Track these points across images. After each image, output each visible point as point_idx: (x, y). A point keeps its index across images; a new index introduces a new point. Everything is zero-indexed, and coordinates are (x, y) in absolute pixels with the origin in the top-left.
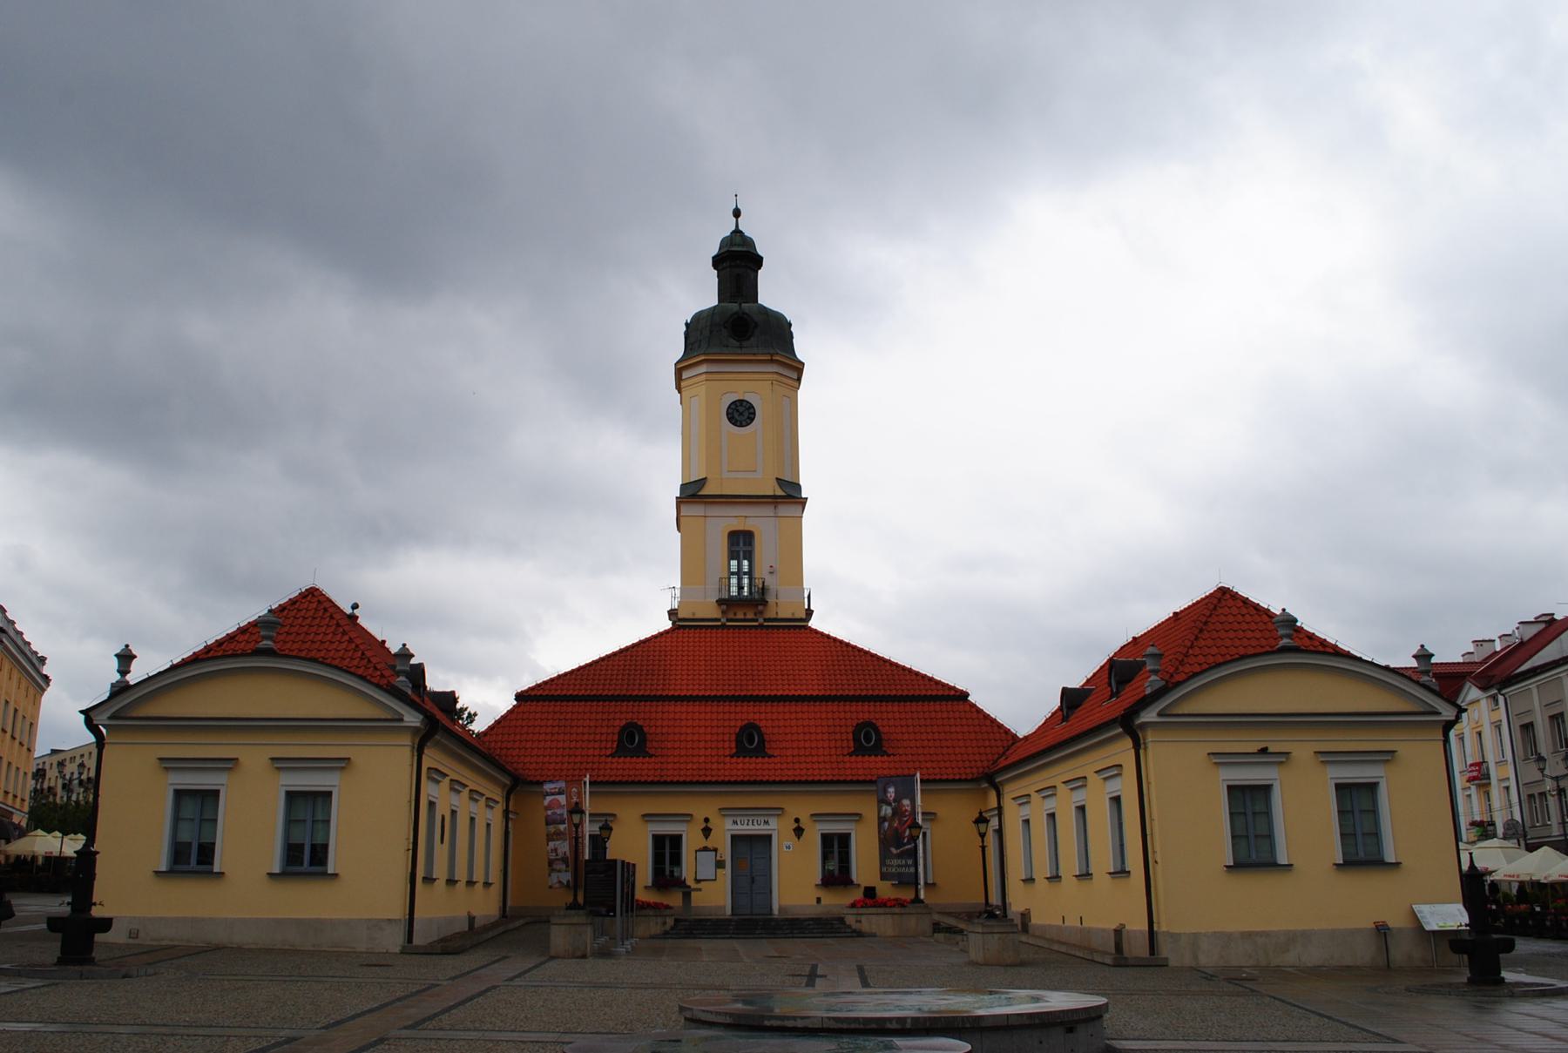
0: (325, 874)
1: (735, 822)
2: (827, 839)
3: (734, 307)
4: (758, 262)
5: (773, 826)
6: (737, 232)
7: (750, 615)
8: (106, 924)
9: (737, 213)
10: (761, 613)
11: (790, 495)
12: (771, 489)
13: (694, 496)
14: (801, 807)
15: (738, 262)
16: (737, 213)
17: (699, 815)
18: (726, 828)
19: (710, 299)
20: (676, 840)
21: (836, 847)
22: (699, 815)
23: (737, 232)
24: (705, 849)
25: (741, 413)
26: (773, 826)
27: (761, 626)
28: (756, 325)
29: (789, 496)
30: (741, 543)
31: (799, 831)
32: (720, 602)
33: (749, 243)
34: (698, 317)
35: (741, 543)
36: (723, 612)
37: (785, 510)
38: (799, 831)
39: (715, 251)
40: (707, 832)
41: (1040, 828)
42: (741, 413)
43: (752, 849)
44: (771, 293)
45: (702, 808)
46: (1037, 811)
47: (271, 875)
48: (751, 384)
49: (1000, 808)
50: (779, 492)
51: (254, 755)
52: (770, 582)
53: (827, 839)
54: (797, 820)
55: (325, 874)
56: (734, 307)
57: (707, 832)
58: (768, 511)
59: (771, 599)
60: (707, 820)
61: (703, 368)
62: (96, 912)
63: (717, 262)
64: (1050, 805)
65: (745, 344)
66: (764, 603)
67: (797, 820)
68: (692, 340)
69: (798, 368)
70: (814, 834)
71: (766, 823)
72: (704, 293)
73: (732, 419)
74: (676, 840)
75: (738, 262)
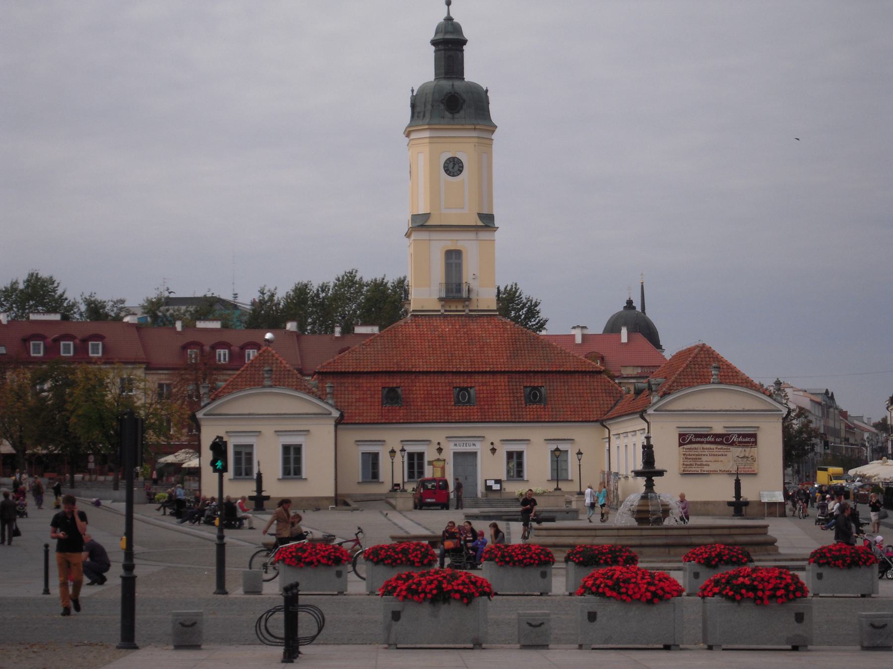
0: (301, 479)
1: (456, 445)
2: (510, 455)
4: (464, 42)
6: (449, 19)
7: (460, 308)
8: (268, 498)
10: (467, 306)
11: (487, 222)
12: (475, 221)
13: (422, 226)
14: (495, 434)
15: (450, 45)
17: (435, 441)
18: (450, 449)
20: (421, 455)
21: (516, 460)
22: (435, 441)
23: (449, 19)
24: (438, 460)
25: (454, 167)
27: (467, 316)
28: (464, 101)
29: (487, 226)
30: (453, 258)
31: (493, 450)
32: (441, 299)
33: (457, 29)
34: (422, 89)
35: (453, 258)
36: (443, 306)
37: (484, 235)
38: (493, 450)
39: (432, 36)
40: (440, 450)
41: (622, 449)
42: (454, 167)
43: (466, 459)
44: (474, 71)
45: (437, 434)
47: (279, 479)
48: (461, 144)
49: (609, 438)
50: (480, 223)
51: (268, 429)
52: (474, 285)
53: (510, 455)
54: (492, 444)
55: (301, 479)
56: (446, 84)
57: (440, 450)
58: (471, 236)
59: (473, 296)
60: (439, 444)
61: (427, 134)
62: (264, 494)
63: (434, 43)
64: (626, 441)
65: (457, 115)
66: (469, 299)
67: (492, 444)
68: (418, 109)
69: (492, 128)
71: (474, 445)
72: (423, 70)
73: (447, 171)
74: (421, 455)
75: (450, 45)
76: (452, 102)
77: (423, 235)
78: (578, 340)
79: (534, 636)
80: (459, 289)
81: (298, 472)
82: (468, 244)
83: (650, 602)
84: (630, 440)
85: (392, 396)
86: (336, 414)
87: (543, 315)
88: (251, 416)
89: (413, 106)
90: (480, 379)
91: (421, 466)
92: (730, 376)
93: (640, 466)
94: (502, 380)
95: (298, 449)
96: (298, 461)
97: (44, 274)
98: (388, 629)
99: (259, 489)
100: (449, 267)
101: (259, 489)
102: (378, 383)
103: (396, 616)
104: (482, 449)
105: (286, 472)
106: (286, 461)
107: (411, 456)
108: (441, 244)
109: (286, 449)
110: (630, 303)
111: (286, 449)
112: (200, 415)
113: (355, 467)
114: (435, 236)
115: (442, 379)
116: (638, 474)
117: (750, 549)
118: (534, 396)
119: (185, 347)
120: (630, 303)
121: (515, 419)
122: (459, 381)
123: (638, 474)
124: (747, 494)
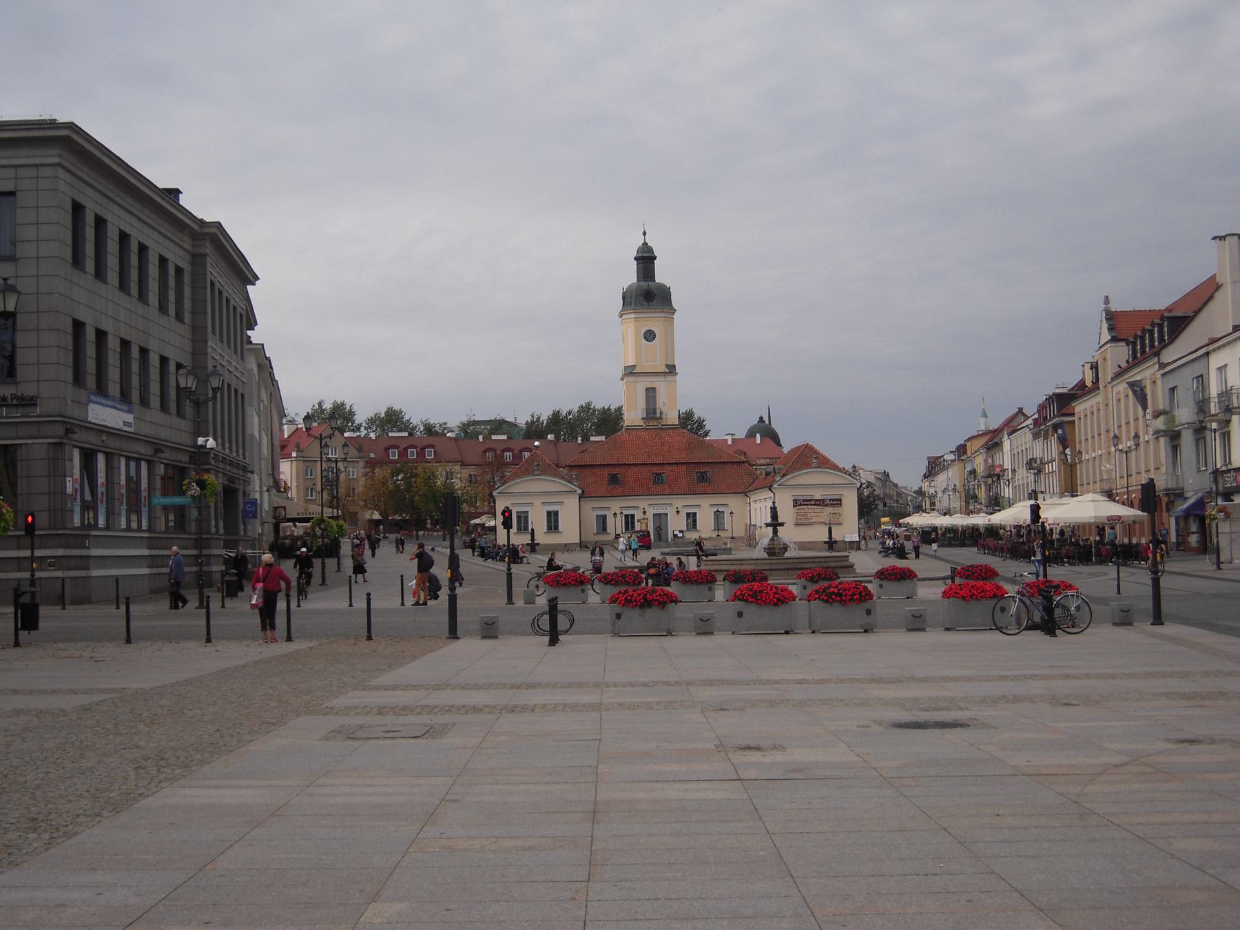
2: (688, 515)
3: (644, 284)
5: (668, 510)
6: (645, 244)
9: (645, 234)
11: (671, 370)
14: (679, 502)
15: (646, 260)
16: (645, 234)
18: (651, 512)
19: (635, 280)
20: (633, 516)
23: (645, 244)
25: (650, 336)
26: (668, 510)
30: (651, 393)
33: (650, 250)
35: (651, 393)
37: (670, 378)
42: (650, 336)
43: (660, 519)
44: (662, 275)
46: (758, 505)
48: (654, 322)
51: (537, 502)
52: (664, 409)
53: (688, 515)
56: (643, 284)
58: (662, 378)
63: (636, 259)
70: (683, 513)
72: (629, 276)
74: (633, 516)
75: (646, 260)
76: (648, 296)
77: (632, 379)
78: (730, 442)
79: (705, 627)
80: (655, 412)
81: (556, 527)
82: (660, 384)
83: (776, 604)
84: (763, 504)
85: (614, 479)
86: (579, 491)
87: (707, 428)
88: (527, 494)
89: (624, 298)
90: (669, 468)
91: (633, 523)
92: (825, 463)
93: (769, 521)
94: (683, 468)
95: (556, 513)
96: (556, 521)
97: (396, 408)
98: (614, 624)
99: (533, 539)
100: (647, 398)
101: (533, 539)
102: (606, 471)
103: (618, 616)
104: (670, 511)
105: (549, 528)
106: (549, 521)
107: (626, 516)
108: (642, 384)
109: (549, 513)
110: (761, 418)
111: (549, 513)
112: (495, 493)
113: (593, 525)
114: (639, 379)
115: (646, 468)
116: (768, 525)
117: (837, 571)
118: (703, 478)
119: (485, 452)
120: (761, 418)
121: (692, 492)
122: (655, 469)
123: (768, 525)
124: (836, 536)
